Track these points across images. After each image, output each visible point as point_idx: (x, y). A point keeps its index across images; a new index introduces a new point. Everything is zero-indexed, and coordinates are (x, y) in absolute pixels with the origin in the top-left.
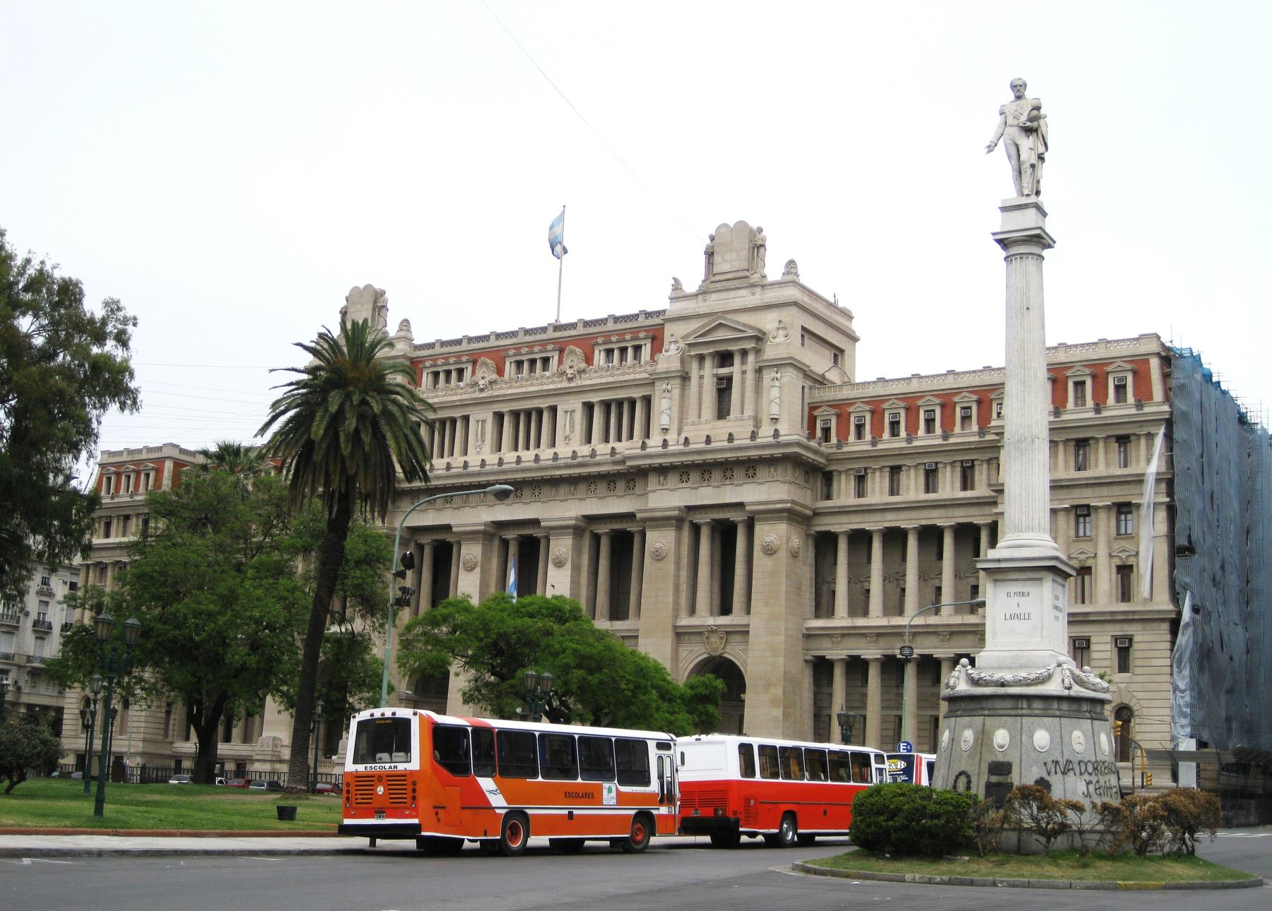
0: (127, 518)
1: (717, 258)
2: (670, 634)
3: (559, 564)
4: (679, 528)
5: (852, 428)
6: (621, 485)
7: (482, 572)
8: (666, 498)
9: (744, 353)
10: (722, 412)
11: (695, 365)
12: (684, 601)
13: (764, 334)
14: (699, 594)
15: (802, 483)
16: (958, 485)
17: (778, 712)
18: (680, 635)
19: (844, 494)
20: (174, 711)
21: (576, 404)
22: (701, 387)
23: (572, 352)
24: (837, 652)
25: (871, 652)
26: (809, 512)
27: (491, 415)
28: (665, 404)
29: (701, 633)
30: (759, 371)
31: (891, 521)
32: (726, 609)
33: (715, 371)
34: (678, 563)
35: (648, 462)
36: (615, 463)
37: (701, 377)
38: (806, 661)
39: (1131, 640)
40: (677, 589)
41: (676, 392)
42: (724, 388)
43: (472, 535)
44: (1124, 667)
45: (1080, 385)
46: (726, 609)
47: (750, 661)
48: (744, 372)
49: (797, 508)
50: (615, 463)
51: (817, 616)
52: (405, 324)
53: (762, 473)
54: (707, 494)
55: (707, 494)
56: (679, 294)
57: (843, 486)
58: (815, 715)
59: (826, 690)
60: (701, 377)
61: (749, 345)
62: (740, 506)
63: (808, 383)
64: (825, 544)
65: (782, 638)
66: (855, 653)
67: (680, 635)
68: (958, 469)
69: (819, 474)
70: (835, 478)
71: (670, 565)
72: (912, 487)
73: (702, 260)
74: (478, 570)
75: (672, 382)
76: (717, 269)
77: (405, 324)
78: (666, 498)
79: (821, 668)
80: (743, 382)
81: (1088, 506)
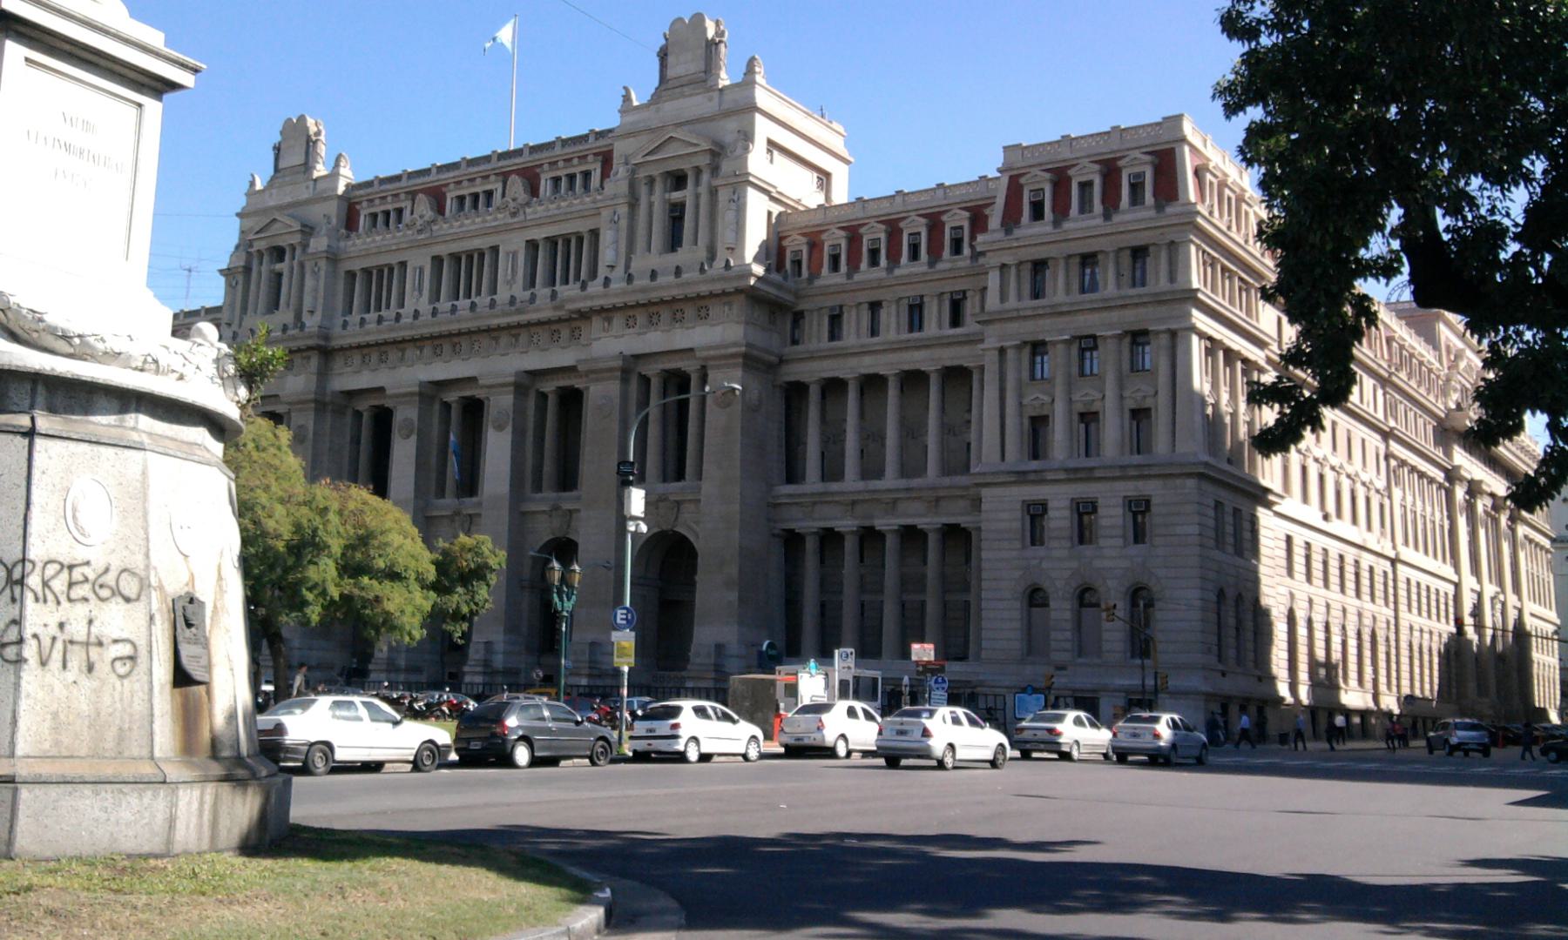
1: (671, 59)
7: (420, 440)
10: (674, 241)
13: (722, 147)
17: (733, 596)
25: (846, 524)
26: (773, 359)
27: (429, 260)
32: (680, 475)
35: (589, 304)
39: (1148, 502)
42: (676, 215)
44: (1139, 536)
45: (1086, 186)
46: (680, 475)
48: (697, 196)
49: (755, 352)
53: (715, 310)
54: (653, 340)
61: (703, 161)
65: (737, 507)
66: (828, 524)
70: (806, 322)
73: (656, 61)
78: (611, 343)
81: (1094, 337)
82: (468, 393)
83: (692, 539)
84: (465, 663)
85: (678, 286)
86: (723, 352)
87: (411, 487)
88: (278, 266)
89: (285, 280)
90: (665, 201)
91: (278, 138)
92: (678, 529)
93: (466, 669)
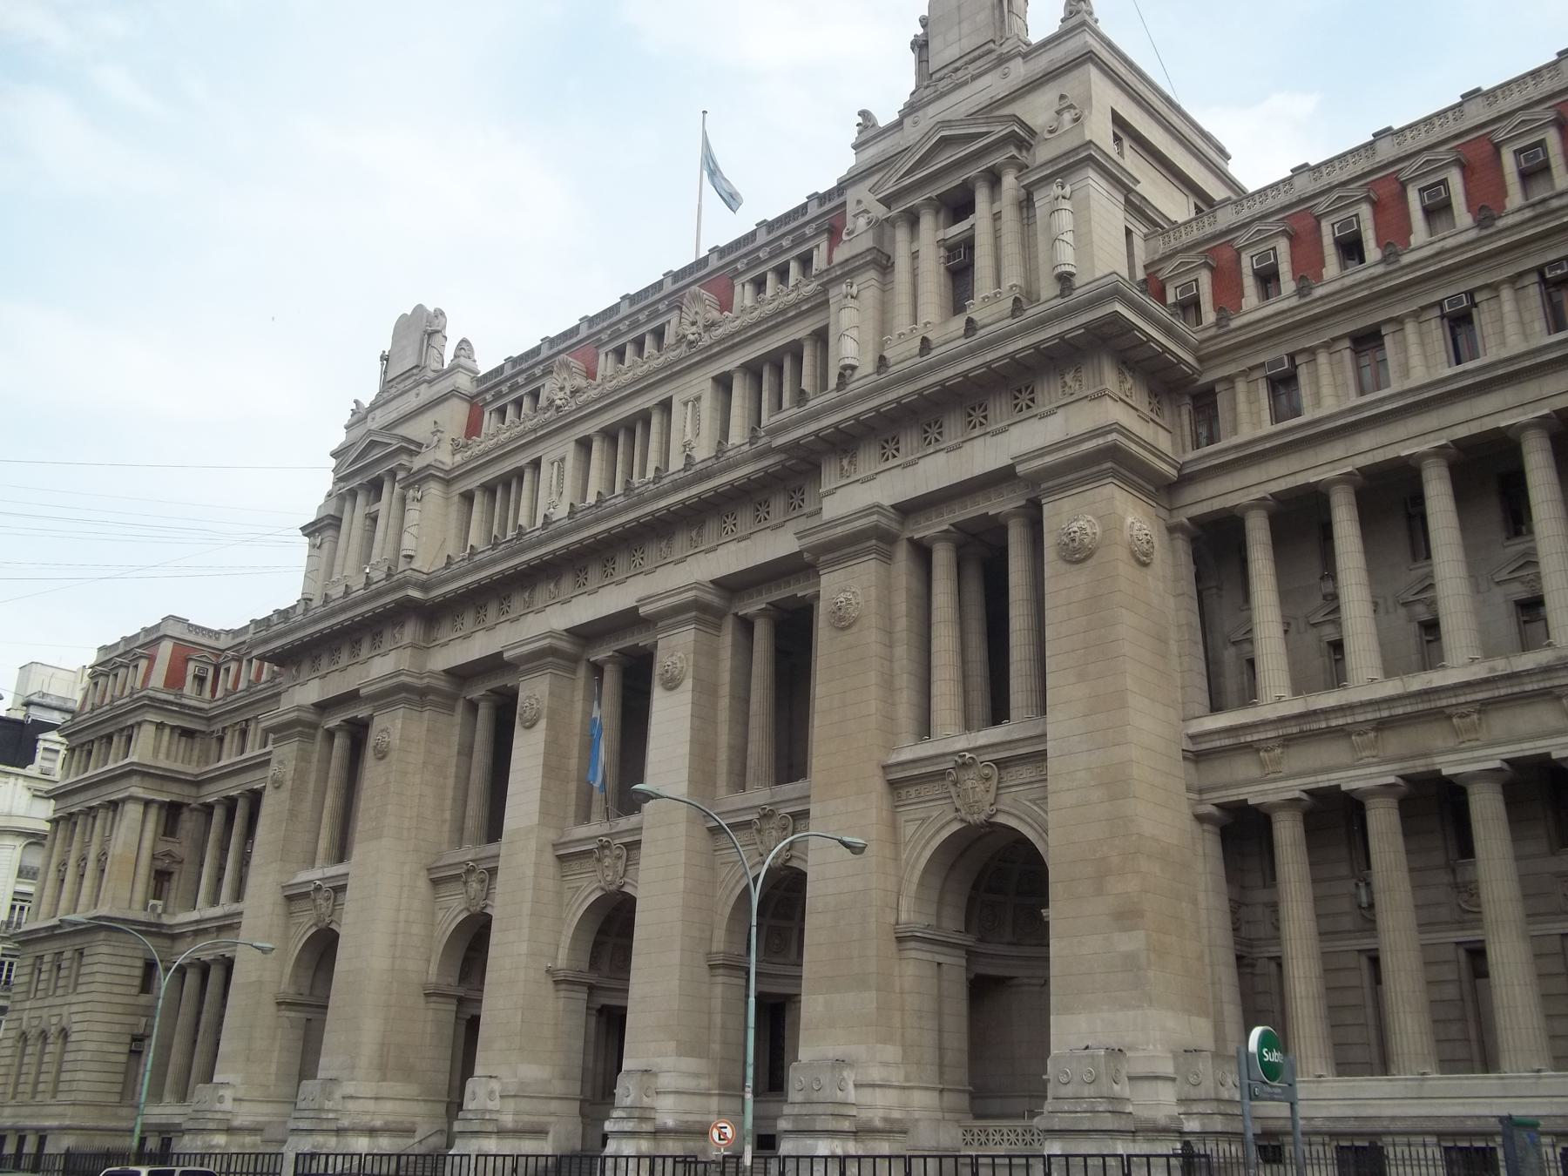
0: (109, 738)
2: (878, 784)
3: (671, 684)
4: (887, 558)
5: (1249, 283)
6: (778, 505)
7: (550, 727)
8: (857, 493)
9: (994, 179)
11: (902, 234)
13: (1032, 132)
14: (936, 689)
15: (1145, 409)
16: (1539, 325)
18: (899, 784)
19: (1249, 416)
21: (701, 383)
23: (696, 298)
29: (942, 775)
30: (1026, 204)
31: (1371, 449)
32: (999, 712)
33: (941, 235)
34: (888, 631)
36: (760, 455)
37: (915, 256)
38: (1200, 819)
40: (888, 685)
41: (870, 295)
43: (539, 658)
46: (999, 712)
47: (1052, 819)
48: (997, 217)
50: (760, 455)
51: (1216, 707)
52: (464, 346)
53: (1049, 393)
56: (871, 133)
57: (1242, 406)
58: (1239, 958)
59: (1262, 895)
60: (915, 256)
62: (1003, 478)
63: (1139, 230)
64: (1215, 548)
66: (1323, 781)
67: (899, 784)
68: (1534, 292)
69: (1186, 393)
70: (1222, 401)
71: (870, 637)
72: (1418, 358)
73: (911, 58)
74: (542, 724)
75: (859, 280)
76: (933, 66)
77: (464, 345)
79: (1242, 833)
82: (627, 642)
84: (608, 1118)
85: (972, 352)
86: (1070, 452)
87: (536, 807)
89: (381, 522)
90: (942, 243)
91: (387, 347)
92: (1001, 819)
93: (608, 1126)
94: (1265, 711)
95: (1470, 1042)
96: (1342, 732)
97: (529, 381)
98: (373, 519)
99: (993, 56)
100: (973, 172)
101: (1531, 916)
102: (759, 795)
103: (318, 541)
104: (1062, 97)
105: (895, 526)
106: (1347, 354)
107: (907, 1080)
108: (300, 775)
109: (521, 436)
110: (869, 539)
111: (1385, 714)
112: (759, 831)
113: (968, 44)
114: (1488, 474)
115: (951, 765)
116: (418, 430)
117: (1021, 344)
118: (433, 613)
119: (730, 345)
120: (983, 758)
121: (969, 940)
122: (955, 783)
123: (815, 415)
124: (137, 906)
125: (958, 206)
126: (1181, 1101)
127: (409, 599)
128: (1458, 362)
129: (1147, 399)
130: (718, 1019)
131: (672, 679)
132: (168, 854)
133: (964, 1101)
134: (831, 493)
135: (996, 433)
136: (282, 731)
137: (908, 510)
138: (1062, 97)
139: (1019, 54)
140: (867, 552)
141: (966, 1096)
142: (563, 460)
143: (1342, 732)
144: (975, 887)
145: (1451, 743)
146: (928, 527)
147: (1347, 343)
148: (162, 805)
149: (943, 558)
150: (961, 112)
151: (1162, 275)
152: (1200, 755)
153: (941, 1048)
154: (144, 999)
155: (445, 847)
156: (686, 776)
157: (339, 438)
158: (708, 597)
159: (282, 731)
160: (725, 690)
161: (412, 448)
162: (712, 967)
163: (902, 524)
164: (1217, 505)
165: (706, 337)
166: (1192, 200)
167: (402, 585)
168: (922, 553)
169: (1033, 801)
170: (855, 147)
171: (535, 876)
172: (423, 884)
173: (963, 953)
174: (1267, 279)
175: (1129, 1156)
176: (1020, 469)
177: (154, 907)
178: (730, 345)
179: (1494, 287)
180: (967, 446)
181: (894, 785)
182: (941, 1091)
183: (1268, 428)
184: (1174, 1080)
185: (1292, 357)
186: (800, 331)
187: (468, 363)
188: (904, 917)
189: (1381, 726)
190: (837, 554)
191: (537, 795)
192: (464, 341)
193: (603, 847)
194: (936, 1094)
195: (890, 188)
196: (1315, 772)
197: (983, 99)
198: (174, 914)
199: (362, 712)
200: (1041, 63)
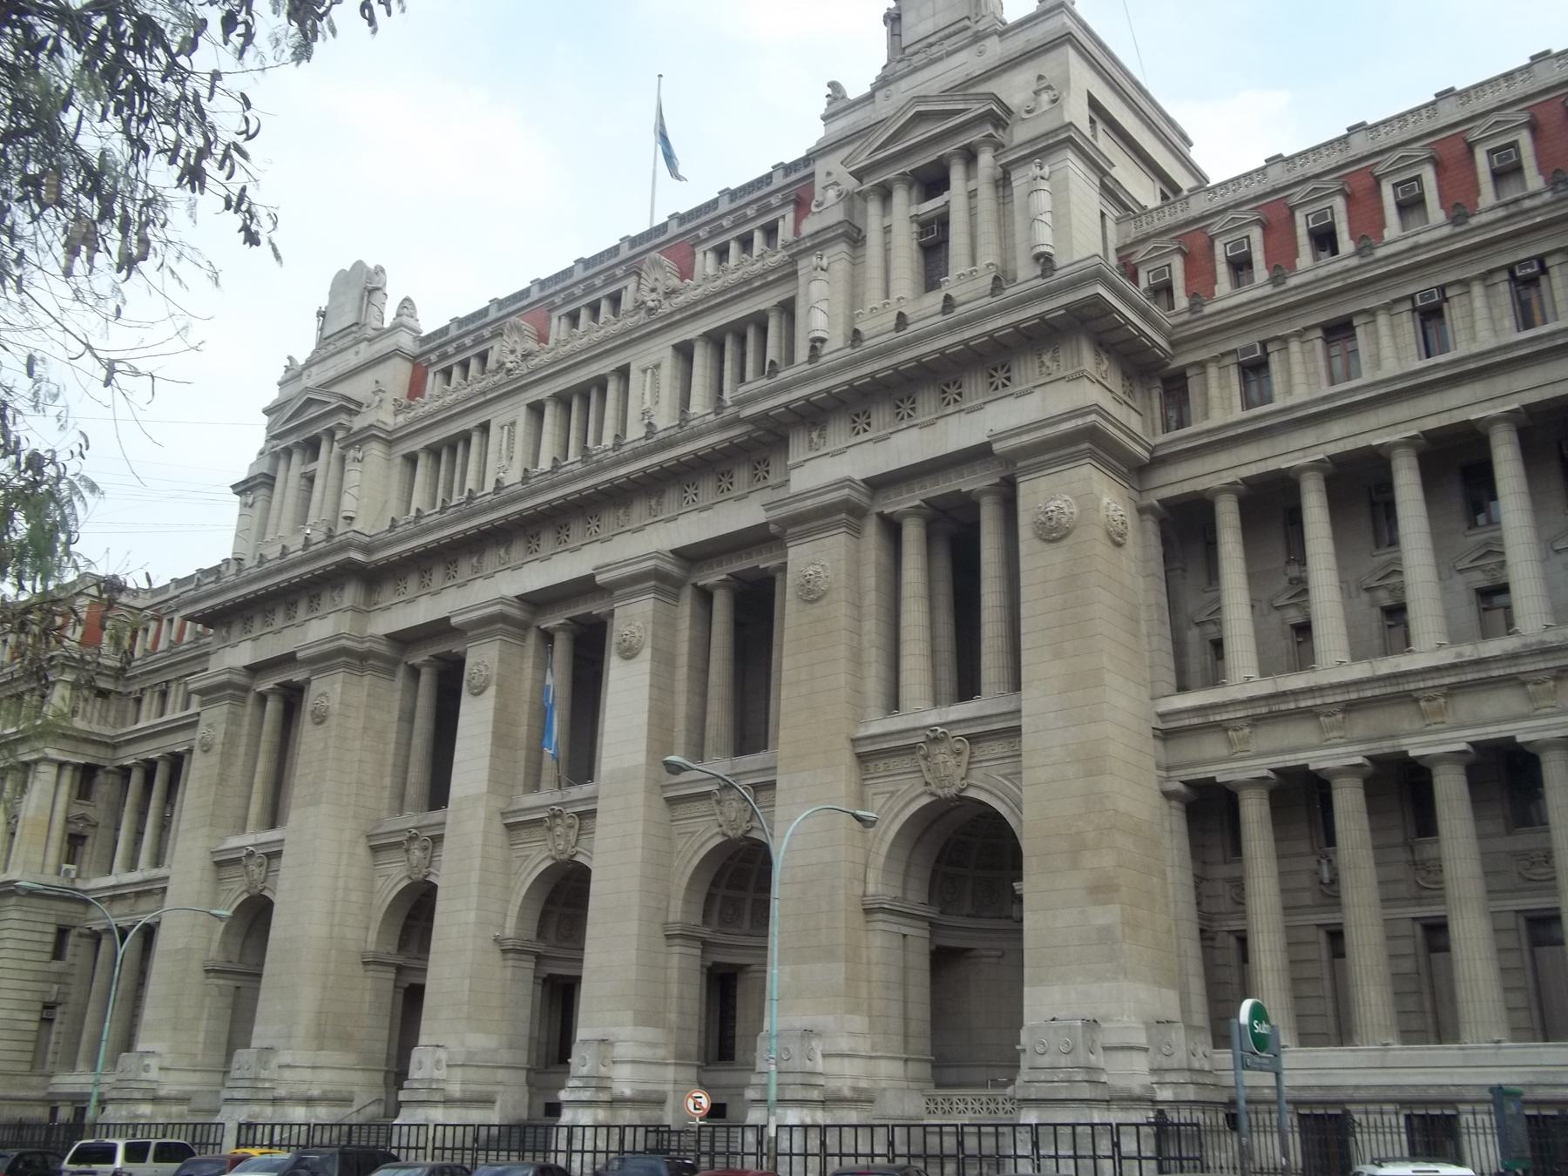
0: (19, 696)
1: (907, 19)
2: (846, 758)
3: (629, 653)
4: (856, 531)
5: (1222, 269)
6: (742, 476)
7: (499, 694)
8: (825, 467)
9: (970, 156)
11: (874, 208)
12: (874, 685)
13: (1009, 111)
15: (1119, 391)
16: (1509, 322)
18: (868, 757)
19: (1220, 402)
20: (58, 1018)
21: (661, 351)
22: (887, 249)
23: (656, 264)
24: (1242, 763)
28: (818, 289)
29: (911, 749)
30: (1003, 182)
31: (1342, 437)
32: (967, 686)
33: (914, 210)
34: (857, 605)
36: (725, 425)
37: (887, 230)
38: (1168, 795)
40: (857, 659)
41: (840, 268)
42: (933, 243)
43: (488, 625)
47: (1027, 795)
48: (972, 195)
50: (725, 425)
51: (1182, 688)
52: (407, 305)
53: (1025, 372)
54: (907, 445)
55: (907, 445)
56: (842, 104)
57: (1214, 391)
58: (1202, 931)
59: (1223, 871)
60: (887, 230)
62: (979, 454)
63: (1112, 212)
64: (1184, 530)
66: (1290, 760)
67: (868, 757)
68: (1503, 289)
69: (1159, 376)
71: (839, 611)
72: (1390, 350)
73: (882, 31)
74: (492, 691)
76: (907, 39)
77: (407, 305)
79: (1209, 811)
80: (972, 213)
82: (579, 610)
83: (1002, 809)
84: (562, 1087)
85: (950, 328)
86: (1049, 432)
87: (485, 775)
88: (311, 467)
89: (318, 482)
90: (914, 218)
91: (324, 302)
92: (971, 793)
93: (563, 1095)
94: (1233, 691)
95: (1430, 1014)
96: (1311, 713)
97: (477, 343)
98: (310, 479)
99: (969, 33)
100: (948, 148)
101: (1491, 893)
102: (720, 766)
103: (250, 500)
104: (1040, 77)
105: (865, 501)
106: (1319, 344)
107: (873, 1048)
108: (230, 740)
109: (469, 399)
110: (840, 512)
111: (1354, 696)
112: (719, 802)
113: (943, 20)
114: (1458, 464)
115: (923, 739)
116: (357, 389)
117: (1000, 322)
118: (374, 577)
119: (693, 313)
120: (955, 733)
121: (932, 912)
122: (926, 758)
123: (786, 387)
124: (50, 870)
125: (933, 182)
126: (1153, 1071)
127: (351, 562)
128: (1428, 356)
129: (1120, 382)
130: (674, 989)
131: (629, 649)
132: (83, 818)
133: (925, 1070)
134: (799, 465)
135: (971, 411)
136: (210, 694)
137: (879, 484)
138: (1040, 77)
139: (996, 32)
140: (837, 525)
141: (929, 1066)
142: (513, 424)
143: (1311, 713)
144: (938, 861)
145: (1418, 725)
146: (898, 503)
147: (1319, 333)
148: (76, 767)
149: (913, 534)
150: (934, 88)
151: (1136, 259)
152: (1169, 733)
153: (906, 1019)
154: (56, 966)
155: (385, 814)
156: (644, 746)
157: (272, 395)
158: (668, 567)
159: (210, 694)
160: (683, 659)
161: (351, 407)
162: (668, 937)
163: (872, 498)
164: (1187, 488)
165: (666, 304)
166: (1158, 185)
167: (344, 547)
168: (892, 528)
169: (1005, 776)
170: (824, 118)
171: (484, 845)
172: (362, 851)
173: (926, 925)
174: (1240, 266)
175: (1118, 1125)
176: (996, 447)
177: (68, 872)
178: (693, 313)
179: (1465, 283)
180: (941, 422)
181: (863, 759)
182: (906, 1060)
183: (1239, 414)
184: (1146, 1050)
185: (1264, 344)
186: (765, 301)
187: (411, 322)
188: (871, 889)
189: (1349, 707)
190: (805, 527)
191: (486, 762)
192: (407, 299)
193: (555, 816)
194: (901, 1063)
195: (862, 161)
196: (1283, 752)
197: (958, 76)
198: (88, 879)
199: (297, 676)
200: (1016, 44)
